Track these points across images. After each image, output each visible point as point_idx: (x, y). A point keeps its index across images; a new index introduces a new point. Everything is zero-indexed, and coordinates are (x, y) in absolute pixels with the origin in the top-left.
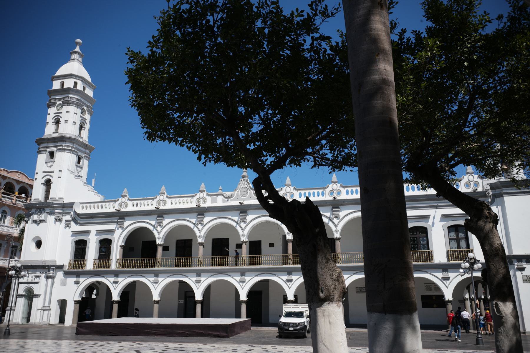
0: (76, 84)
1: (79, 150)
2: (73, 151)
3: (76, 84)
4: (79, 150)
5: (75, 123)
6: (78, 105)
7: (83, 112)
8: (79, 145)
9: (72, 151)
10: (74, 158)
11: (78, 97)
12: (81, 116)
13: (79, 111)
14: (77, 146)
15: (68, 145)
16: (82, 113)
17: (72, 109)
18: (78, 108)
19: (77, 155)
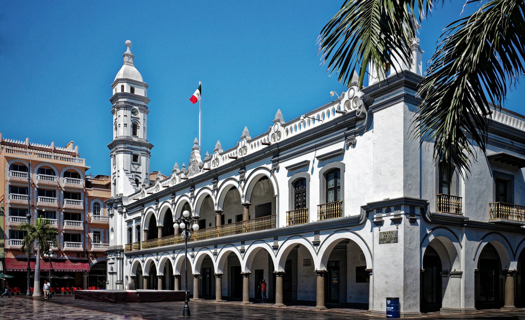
0: (123, 87)
1: (132, 149)
2: (126, 151)
3: (123, 87)
4: (132, 149)
5: (126, 124)
6: (126, 108)
7: (134, 112)
8: (132, 145)
9: (125, 152)
10: (129, 157)
11: (125, 100)
12: (132, 117)
13: (129, 113)
14: (130, 146)
15: (121, 147)
16: (132, 113)
17: (121, 112)
18: (126, 109)
19: (131, 154)
